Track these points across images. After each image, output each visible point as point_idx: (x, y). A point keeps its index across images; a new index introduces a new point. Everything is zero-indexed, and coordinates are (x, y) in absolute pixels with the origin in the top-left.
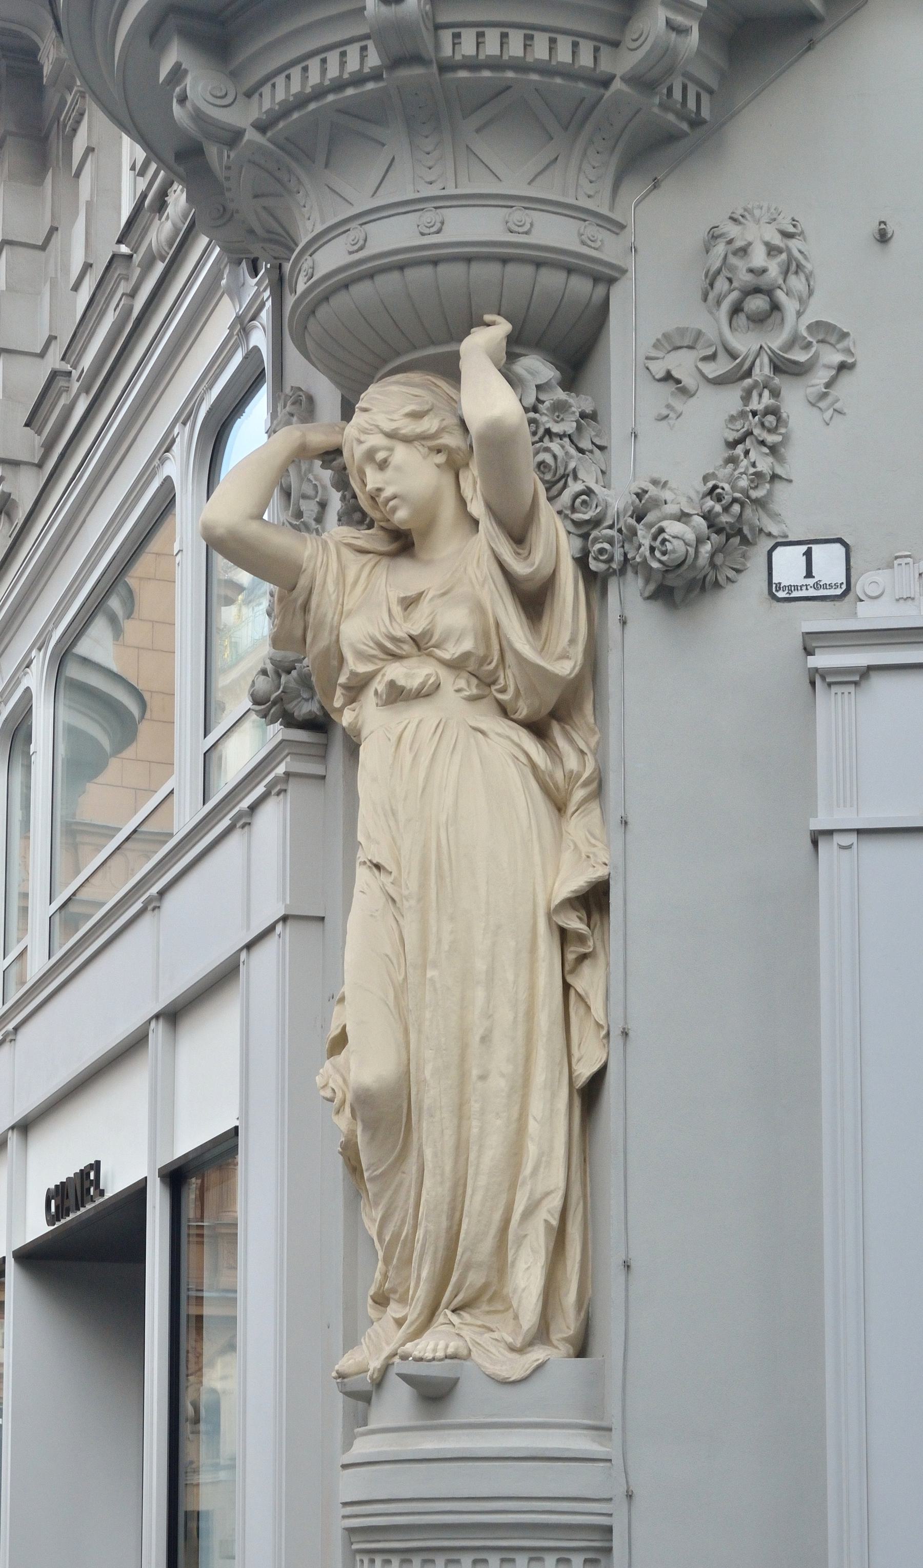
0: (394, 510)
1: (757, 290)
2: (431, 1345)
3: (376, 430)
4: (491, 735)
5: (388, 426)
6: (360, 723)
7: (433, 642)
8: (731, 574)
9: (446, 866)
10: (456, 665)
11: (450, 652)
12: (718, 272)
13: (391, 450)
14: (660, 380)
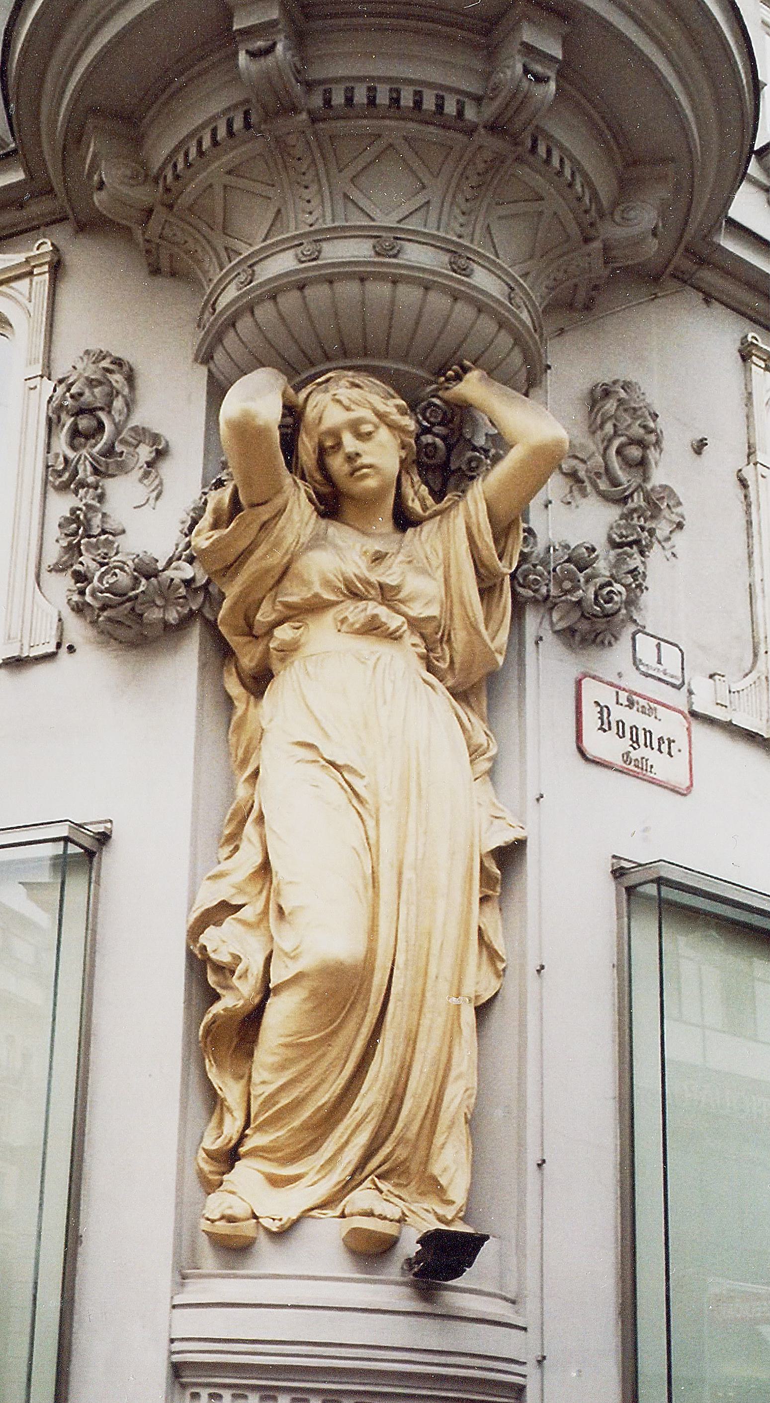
0: (365, 476)
10: (414, 624)
11: (416, 610)
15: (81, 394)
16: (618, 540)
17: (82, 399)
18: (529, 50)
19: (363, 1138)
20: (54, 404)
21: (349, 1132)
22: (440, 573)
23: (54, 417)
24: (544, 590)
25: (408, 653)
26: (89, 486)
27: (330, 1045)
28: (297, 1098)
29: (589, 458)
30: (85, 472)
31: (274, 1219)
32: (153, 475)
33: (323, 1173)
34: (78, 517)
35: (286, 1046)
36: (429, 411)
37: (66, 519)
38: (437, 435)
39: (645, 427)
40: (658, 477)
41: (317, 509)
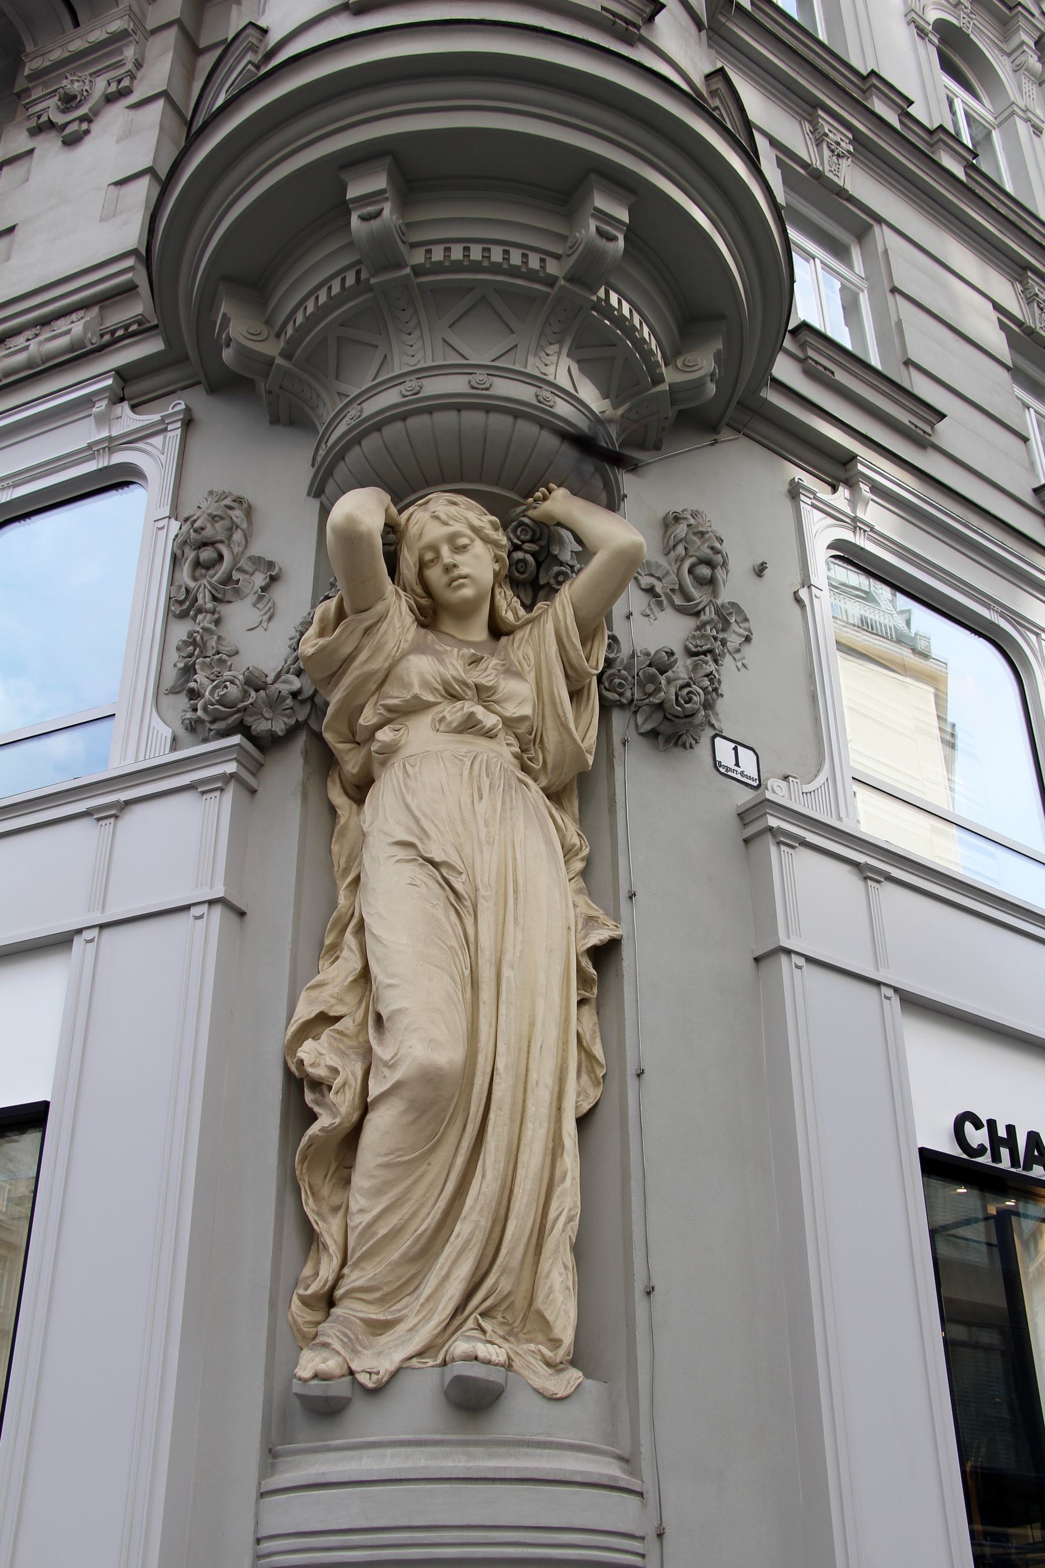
1: (709, 563)
2: (481, 1348)
3: (464, 521)
4: (533, 790)
5: (477, 523)
6: (403, 742)
7: (494, 698)
8: (693, 742)
9: (520, 882)
10: (509, 723)
11: (512, 710)
12: (681, 541)
13: (472, 541)
14: (643, 590)
15: (203, 529)
16: (694, 649)
17: (204, 533)
18: (602, 215)
19: (464, 1270)
20: (179, 540)
21: (449, 1263)
22: (531, 677)
23: (179, 553)
24: (628, 694)
25: (502, 752)
26: (207, 612)
27: (429, 1164)
28: (395, 1225)
29: (664, 577)
30: (204, 599)
31: (370, 1373)
32: (265, 600)
33: (423, 1313)
34: (195, 639)
35: (381, 1166)
36: (519, 530)
37: (184, 642)
38: (526, 552)
39: (712, 548)
40: (725, 596)
41: (417, 619)
